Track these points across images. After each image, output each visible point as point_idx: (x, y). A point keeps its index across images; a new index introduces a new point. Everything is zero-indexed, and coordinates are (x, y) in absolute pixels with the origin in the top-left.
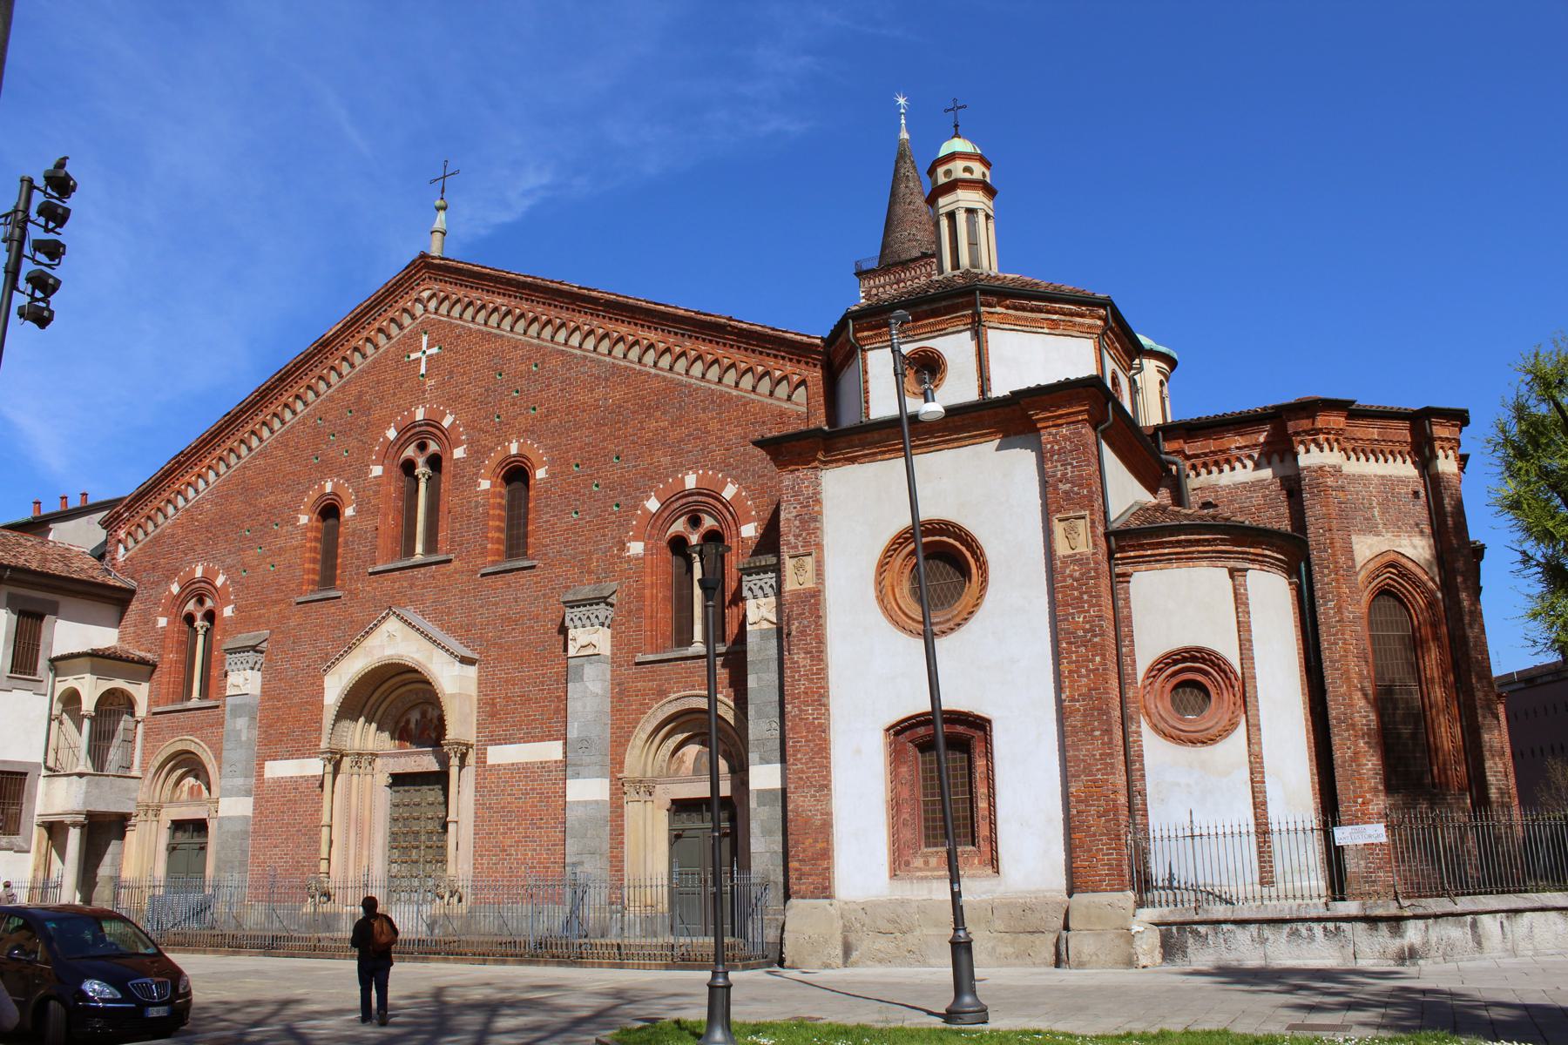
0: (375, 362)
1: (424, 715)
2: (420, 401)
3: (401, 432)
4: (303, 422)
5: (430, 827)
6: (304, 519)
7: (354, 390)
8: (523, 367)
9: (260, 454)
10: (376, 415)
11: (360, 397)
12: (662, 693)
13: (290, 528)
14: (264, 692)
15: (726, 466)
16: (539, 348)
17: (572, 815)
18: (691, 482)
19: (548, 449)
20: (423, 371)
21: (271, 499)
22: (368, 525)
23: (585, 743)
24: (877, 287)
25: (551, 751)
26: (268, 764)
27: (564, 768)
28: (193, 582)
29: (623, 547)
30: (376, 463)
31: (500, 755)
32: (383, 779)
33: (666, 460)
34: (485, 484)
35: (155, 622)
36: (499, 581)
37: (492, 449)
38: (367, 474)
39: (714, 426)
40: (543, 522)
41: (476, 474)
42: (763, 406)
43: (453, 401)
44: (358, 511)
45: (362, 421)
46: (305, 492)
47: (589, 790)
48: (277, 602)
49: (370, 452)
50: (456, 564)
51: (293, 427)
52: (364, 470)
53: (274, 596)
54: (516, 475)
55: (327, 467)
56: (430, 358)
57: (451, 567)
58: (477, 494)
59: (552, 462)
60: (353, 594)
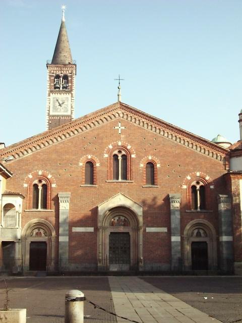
0: (103, 127)
1: (119, 218)
2: (120, 139)
3: (114, 146)
4: (78, 137)
5: (122, 245)
6: (81, 164)
7: (96, 132)
8: (152, 139)
9: (62, 143)
10: (105, 141)
11: (98, 135)
12: (192, 219)
13: (76, 166)
14: (70, 209)
15: (207, 173)
16: (156, 135)
17: (173, 245)
18: (198, 174)
19: (160, 160)
20: (120, 132)
21: (67, 156)
22: (105, 169)
23: (176, 228)
24: (54, 71)
25: (165, 230)
26: (73, 228)
27: (170, 233)
28: (37, 174)
29: (181, 186)
30: (106, 153)
31: (149, 230)
32: (108, 233)
33: (192, 168)
34: (142, 165)
35: (22, 186)
36: (148, 189)
37: (144, 157)
38: (103, 156)
39: (203, 163)
40: (159, 177)
41: (139, 162)
42: (215, 161)
43: (131, 143)
44: (102, 164)
45: (100, 141)
46: (81, 157)
47: (175, 239)
48: (73, 185)
49: (104, 150)
50: (134, 184)
51: (74, 138)
52: (101, 154)
53: (72, 184)
54: (151, 165)
55: (87, 151)
56: (121, 130)
57: (133, 184)
58: (140, 167)
59: (161, 163)
60: (101, 187)
